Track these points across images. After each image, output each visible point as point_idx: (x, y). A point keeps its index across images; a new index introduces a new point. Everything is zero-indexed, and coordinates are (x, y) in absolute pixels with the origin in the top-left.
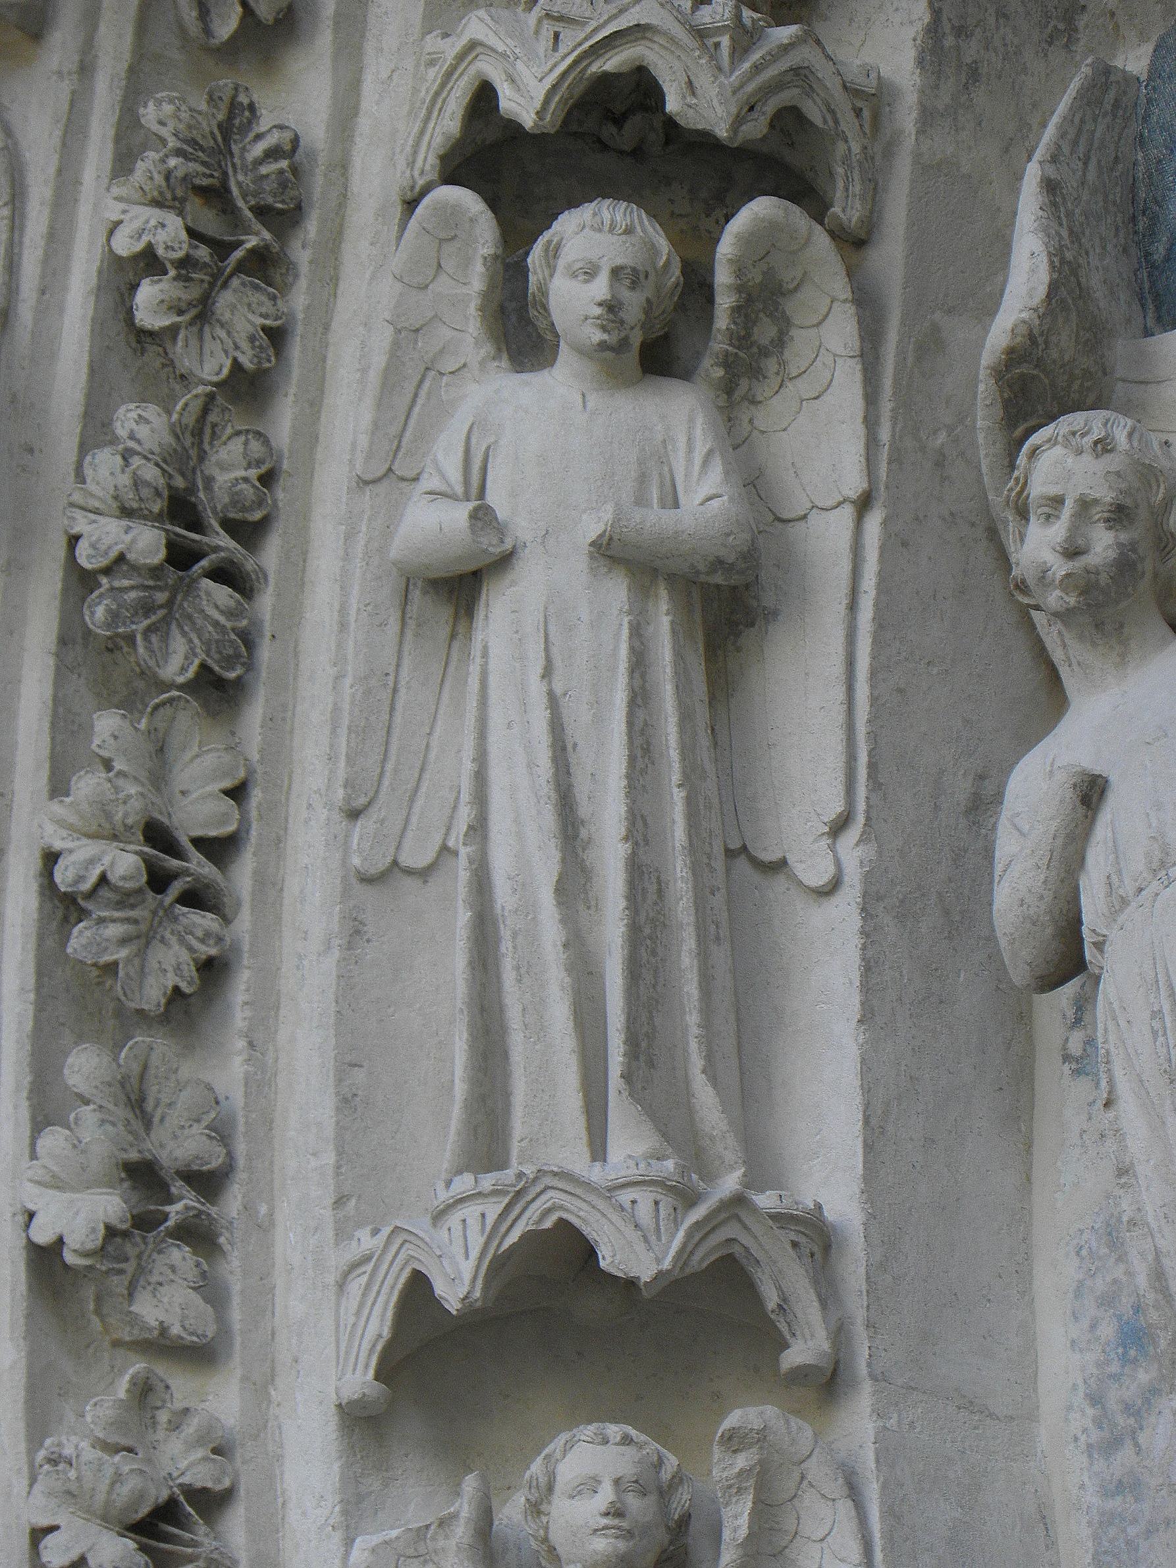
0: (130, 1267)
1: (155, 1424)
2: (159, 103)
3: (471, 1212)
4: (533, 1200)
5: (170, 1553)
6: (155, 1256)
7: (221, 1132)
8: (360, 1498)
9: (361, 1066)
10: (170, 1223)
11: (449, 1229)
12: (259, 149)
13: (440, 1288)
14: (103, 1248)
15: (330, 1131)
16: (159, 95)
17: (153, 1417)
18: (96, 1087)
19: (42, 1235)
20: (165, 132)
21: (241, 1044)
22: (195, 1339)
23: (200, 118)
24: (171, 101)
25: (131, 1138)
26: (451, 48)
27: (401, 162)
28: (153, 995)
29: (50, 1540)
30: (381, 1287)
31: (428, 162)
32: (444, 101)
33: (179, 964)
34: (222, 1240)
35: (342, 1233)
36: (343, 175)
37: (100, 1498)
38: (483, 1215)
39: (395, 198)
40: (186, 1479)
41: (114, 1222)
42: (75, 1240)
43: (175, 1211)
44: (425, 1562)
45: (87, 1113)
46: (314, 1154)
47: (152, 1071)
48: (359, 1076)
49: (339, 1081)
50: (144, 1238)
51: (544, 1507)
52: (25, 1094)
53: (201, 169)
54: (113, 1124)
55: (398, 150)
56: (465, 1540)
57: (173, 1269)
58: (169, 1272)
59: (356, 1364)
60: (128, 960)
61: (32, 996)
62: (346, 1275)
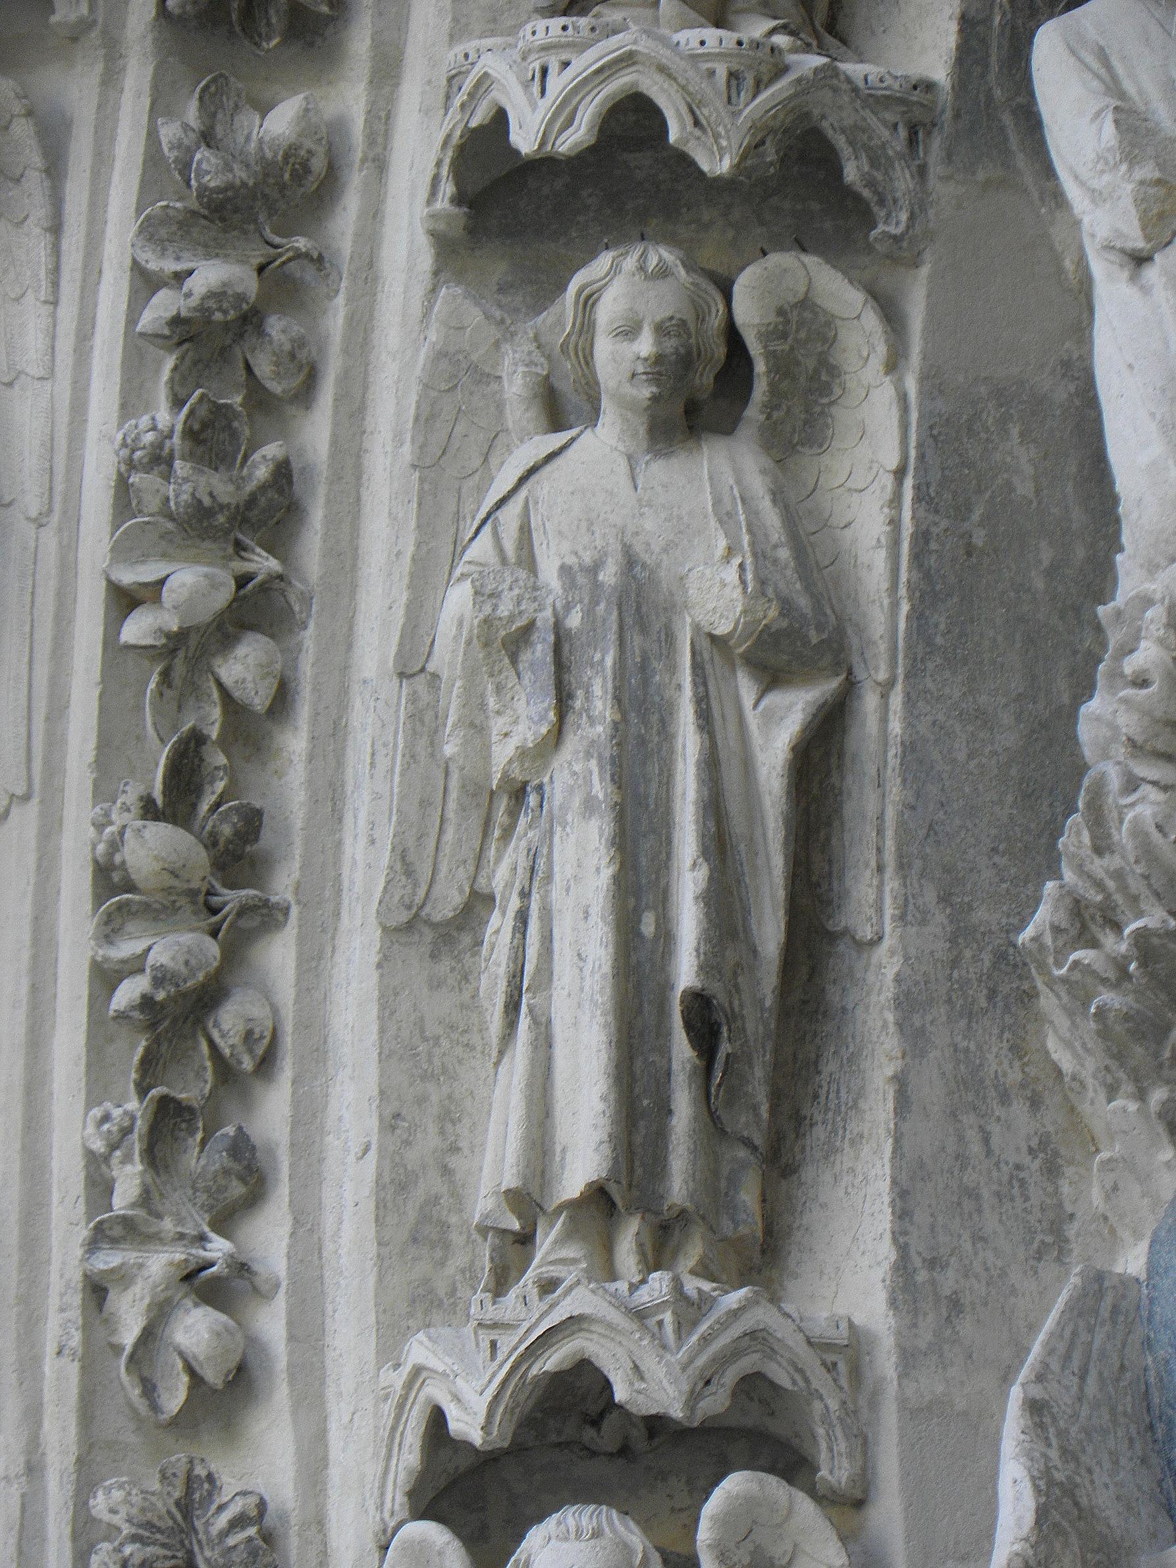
2: (108, 1491)
12: (223, 1520)
16: (108, 1483)
20: (117, 1520)
23: (154, 1499)
24: (121, 1486)
26: (397, 1379)
27: (371, 1504)
31: (397, 1499)
32: (402, 1433)
36: (320, 1531)
39: (371, 1545)
53: (161, 1552)
55: (368, 1496)
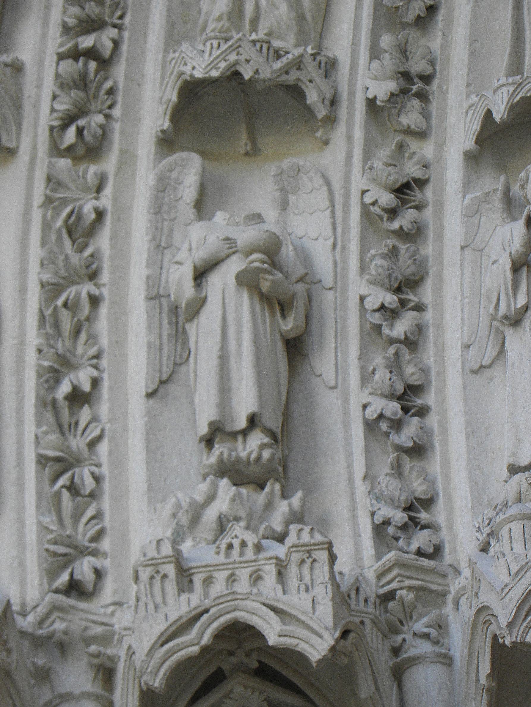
0: (399, 106)
1: (404, 157)
3: (505, 90)
4: (525, 86)
5: (406, 199)
6: (408, 102)
7: (432, 63)
8: (469, 182)
9: (477, 41)
10: (413, 92)
11: (498, 95)
13: (494, 115)
14: (389, 100)
15: (466, 62)
17: (404, 155)
18: (390, 47)
19: (370, 96)
21: (440, 33)
22: (419, 130)
25: (401, 64)
28: (411, 17)
29: (367, 194)
30: (478, 113)
33: (420, 7)
34: (430, 97)
35: (468, 96)
37: (384, 181)
38: (509, 91)
40: (413, 175)
41: (393, 91)
42: (379, 97)
43: (415, 88)
44: (488, 204)
45: (387, 56)
46: (461, 70)
47: (409, 42)
48: (477, 44)
49: (470, 46)
50: (404, 97)
51: (525, 187)
52: (368, 49)
54: (395, 59)
56: (500, 197)
57: (413, 107)
58: (411, 107)
59: (469, 139)
60: (403, 6)
61: (372, 17)
62: (468, 109)
